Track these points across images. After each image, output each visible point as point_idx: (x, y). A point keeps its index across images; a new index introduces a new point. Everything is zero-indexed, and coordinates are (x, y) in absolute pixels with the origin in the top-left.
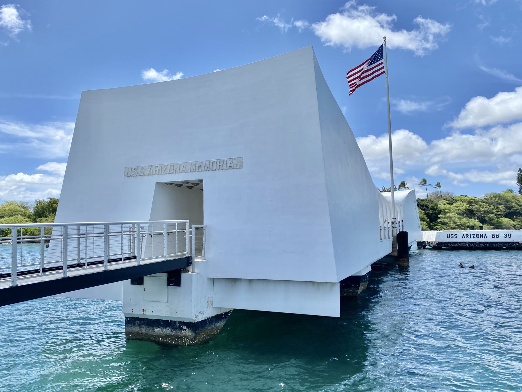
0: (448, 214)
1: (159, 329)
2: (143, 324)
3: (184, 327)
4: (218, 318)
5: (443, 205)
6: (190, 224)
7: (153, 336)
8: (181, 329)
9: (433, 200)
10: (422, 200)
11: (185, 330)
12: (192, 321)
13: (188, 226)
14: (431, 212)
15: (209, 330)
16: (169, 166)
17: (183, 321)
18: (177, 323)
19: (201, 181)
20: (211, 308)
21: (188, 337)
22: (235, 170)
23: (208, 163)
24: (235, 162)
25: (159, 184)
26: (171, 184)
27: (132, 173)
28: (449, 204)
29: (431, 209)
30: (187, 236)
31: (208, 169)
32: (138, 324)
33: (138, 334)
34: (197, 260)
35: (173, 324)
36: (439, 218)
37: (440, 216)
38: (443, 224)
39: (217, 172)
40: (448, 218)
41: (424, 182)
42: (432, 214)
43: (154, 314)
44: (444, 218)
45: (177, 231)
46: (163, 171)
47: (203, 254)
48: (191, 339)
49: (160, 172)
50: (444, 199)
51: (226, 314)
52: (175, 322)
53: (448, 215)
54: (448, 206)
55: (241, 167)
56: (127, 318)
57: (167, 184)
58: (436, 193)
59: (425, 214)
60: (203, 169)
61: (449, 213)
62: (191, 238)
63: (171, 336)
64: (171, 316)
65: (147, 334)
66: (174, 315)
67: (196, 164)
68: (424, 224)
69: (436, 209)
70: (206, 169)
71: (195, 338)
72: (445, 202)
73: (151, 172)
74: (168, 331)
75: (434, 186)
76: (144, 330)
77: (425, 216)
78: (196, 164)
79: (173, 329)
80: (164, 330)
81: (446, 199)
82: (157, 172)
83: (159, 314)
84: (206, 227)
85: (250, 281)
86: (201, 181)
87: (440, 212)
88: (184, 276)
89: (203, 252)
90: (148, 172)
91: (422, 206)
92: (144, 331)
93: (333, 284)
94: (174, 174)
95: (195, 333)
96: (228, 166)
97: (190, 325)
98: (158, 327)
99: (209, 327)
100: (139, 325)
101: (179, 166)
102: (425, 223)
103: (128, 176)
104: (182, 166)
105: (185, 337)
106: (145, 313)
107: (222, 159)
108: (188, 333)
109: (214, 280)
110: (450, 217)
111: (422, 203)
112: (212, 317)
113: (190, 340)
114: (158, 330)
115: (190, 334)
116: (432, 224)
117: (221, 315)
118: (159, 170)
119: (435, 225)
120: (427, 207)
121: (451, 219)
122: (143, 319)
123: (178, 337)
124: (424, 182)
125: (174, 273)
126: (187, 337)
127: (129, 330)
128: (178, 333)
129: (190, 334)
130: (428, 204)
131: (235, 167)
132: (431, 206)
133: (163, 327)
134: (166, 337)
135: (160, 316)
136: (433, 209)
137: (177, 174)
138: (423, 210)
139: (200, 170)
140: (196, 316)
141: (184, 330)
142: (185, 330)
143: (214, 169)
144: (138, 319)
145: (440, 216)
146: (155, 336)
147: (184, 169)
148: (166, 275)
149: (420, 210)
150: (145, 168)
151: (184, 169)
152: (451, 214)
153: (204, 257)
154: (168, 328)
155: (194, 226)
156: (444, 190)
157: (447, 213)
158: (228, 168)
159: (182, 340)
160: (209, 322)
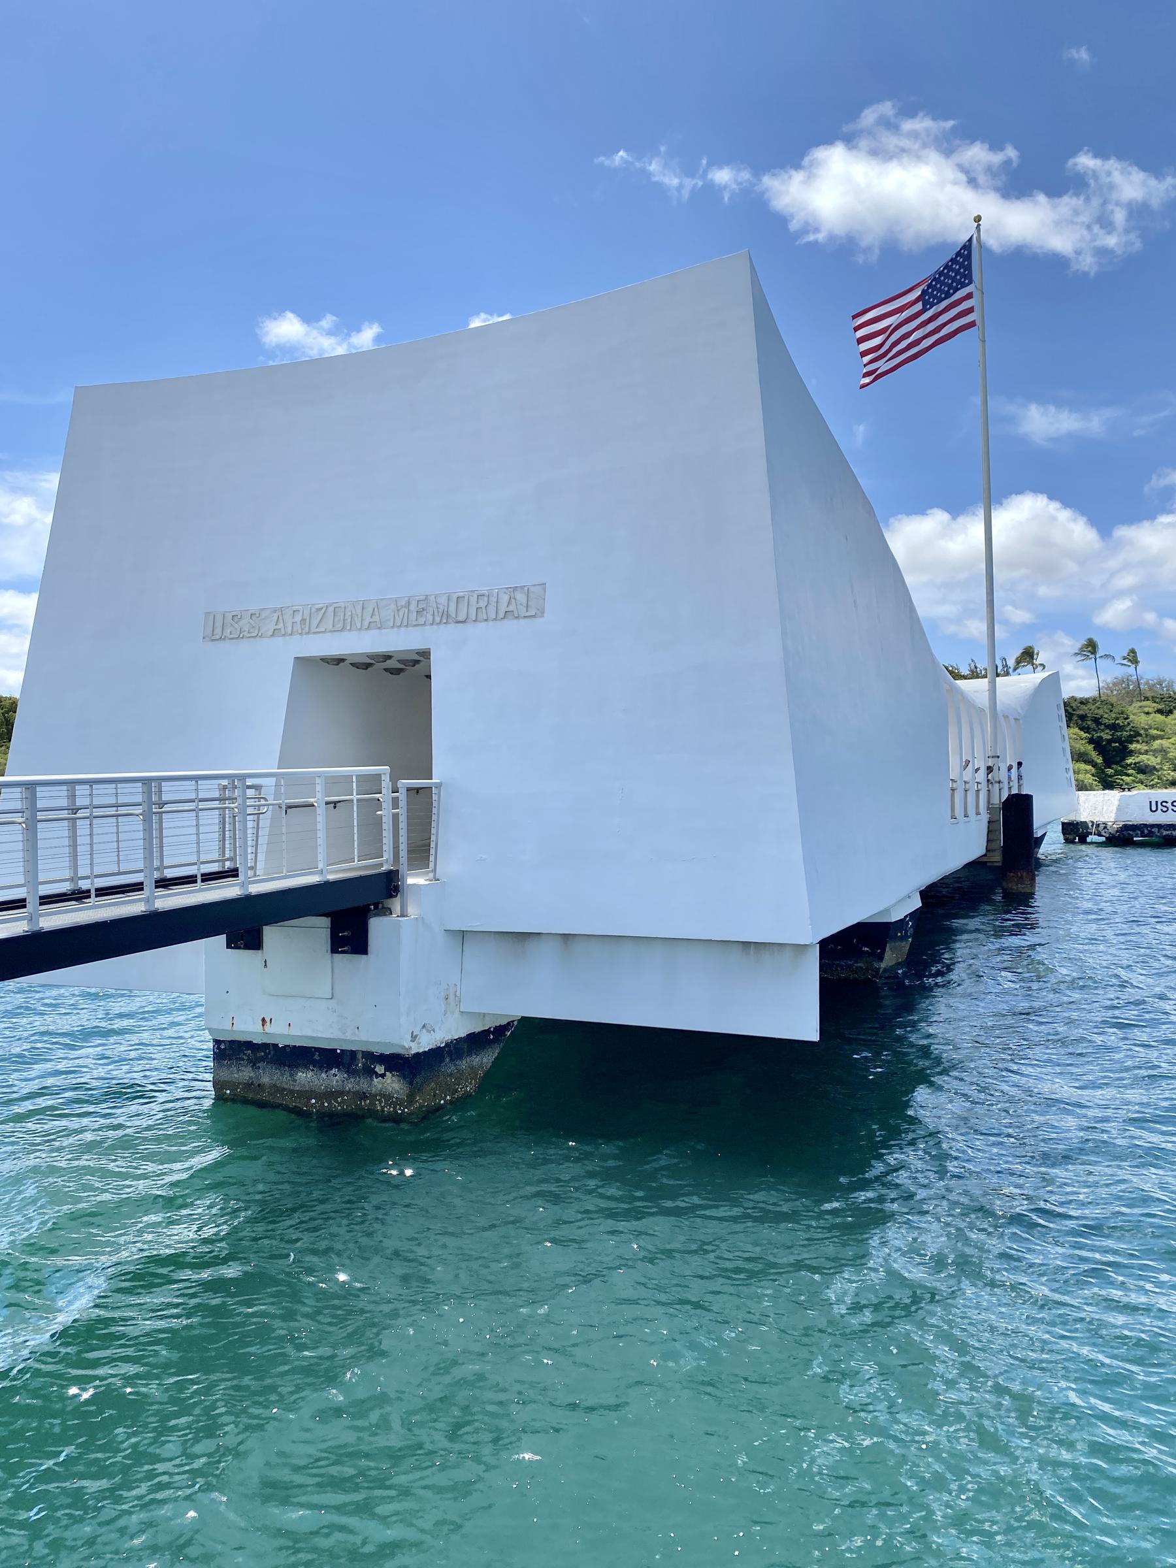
0: (1158, 742)
1: (310, 1074)
2: (262, 1059)
3: (380, 1069)
4: (475, 1042)
5: (1143, 718)
6: (394, 779)
7: (292, 1092)
8: (371, 1073)
9: (1113, 700)
10: (1084, 702)
11: (383, 1076)
12: (402, 1052)
13: (386, 784)
14: (1106, 735)
15: (451, 1075)
16: (331, 609)
17: (377, 1050)
18: (360, 1056)
19: (426, 654)
20: (457, 1014)
22: (522, 622)
23: (443, 600)
24: (521, 597)
26: (339, 661)
28: (1160, 711)
29: (1108, 727)
30: (386, 813)
31: (446, 618)
32: (250, 1061)
33: (249, 1085)
34: (414, 880)
35: (346, 1059)
36: (1131, 753)
37: (1133, 746)
38: (1143, 770)
39: (469, 628)
40: (1155, 752)
41: (1091, 647)
42: (1109, 742)
43: (295, 1031)
44: (1146, 752)
45: (355, 797)
46: (315, 623)
47: (432, 865)
48: (399, 1102)
49: (306, 628)
50: (1147, 699)
51: (500, 1030)
52: (353, 1054)
53: (1157, 744)
54: (1159, 717)
55: (541, 612)
56: (217, 1042)
57: (326, 660)
58: (1125, 681)
59: (1091, 741)
60: (430, 618)
61: (1162, 737)
62: (396, 817)
63: (341, 1093)
64: (341, 1036)
65: (275, 1085)
66: (349, 1036)
67: (409, 603)
68: (1086, 772)
69: (1122, 728)
70: (438, 619)
71: (411, 1098)
72: (1151, 706)
73: (281, 626)
74: (334, 1079)
75: (1118, 660)
76: (268, 1076)
77: (1091, 747)
79: (348, 1072)
80: (323, 1075)
81: (1154, 700)
82: (298, 627)
83: (308, 1032)
84: (438, 786)
85: (567, 938)
86: (426, 654)
87: (1135, 736)
88: (377, 926)
89: (432, 858)
90: (272, 627)
91: (1083, 717)
92: (265, 1080)
93: (800, 948)
94: (345, 634)
95: (411, 1083)
96: (503, 608)
97: (396, 1062)
98: (306, 1067)
99: (449, 1067)
100: (253, 1063)
102: (1089, 767)
103: (212, 637)
105: (380, 1095)
106: (268, 1028)
107: (484, 590)
108: (391, 1083)
109: (462, 936)
110: (1163, 751)
111: (1083, 710)
112: (459, 1040)
113: (395, 1104)
114: (305, 1077)
115: (396, 1086)
116: (1110, 771)
117: (487, 1032)
118: (303, 620)
119: (1117, 773)
120: (1097, 721)
121: (1165, 758)
122: (265, 1046)
123: (363, 1096)
124: (1091, 647)
125: (349, 915)
126: (387, 1097)
127: (225, 1075)
128: (362, 1084)
130: (1100, 712)
131: (523, 612)
132: (1109, 718)
133: (321, 1068)
134: (331, 1095)
136: (1114, 727)
138: (1086, 729)
139: (422, 620)
140: (414, 1038)
141: (378, 1075)
142: (383, 1076)
143: (460, 618)
144: (249, 1045)
145: (1133, 746)
147: (376, 618)
148: (325, 922)
149: (1076, 730)
151: (376, 618)
152: (1165, 743)
153: (434, 871)
155: (404, 783)
156: (1148, 671)
157: (1155, 738)
158: (501, 615)
160: (450, 1053)
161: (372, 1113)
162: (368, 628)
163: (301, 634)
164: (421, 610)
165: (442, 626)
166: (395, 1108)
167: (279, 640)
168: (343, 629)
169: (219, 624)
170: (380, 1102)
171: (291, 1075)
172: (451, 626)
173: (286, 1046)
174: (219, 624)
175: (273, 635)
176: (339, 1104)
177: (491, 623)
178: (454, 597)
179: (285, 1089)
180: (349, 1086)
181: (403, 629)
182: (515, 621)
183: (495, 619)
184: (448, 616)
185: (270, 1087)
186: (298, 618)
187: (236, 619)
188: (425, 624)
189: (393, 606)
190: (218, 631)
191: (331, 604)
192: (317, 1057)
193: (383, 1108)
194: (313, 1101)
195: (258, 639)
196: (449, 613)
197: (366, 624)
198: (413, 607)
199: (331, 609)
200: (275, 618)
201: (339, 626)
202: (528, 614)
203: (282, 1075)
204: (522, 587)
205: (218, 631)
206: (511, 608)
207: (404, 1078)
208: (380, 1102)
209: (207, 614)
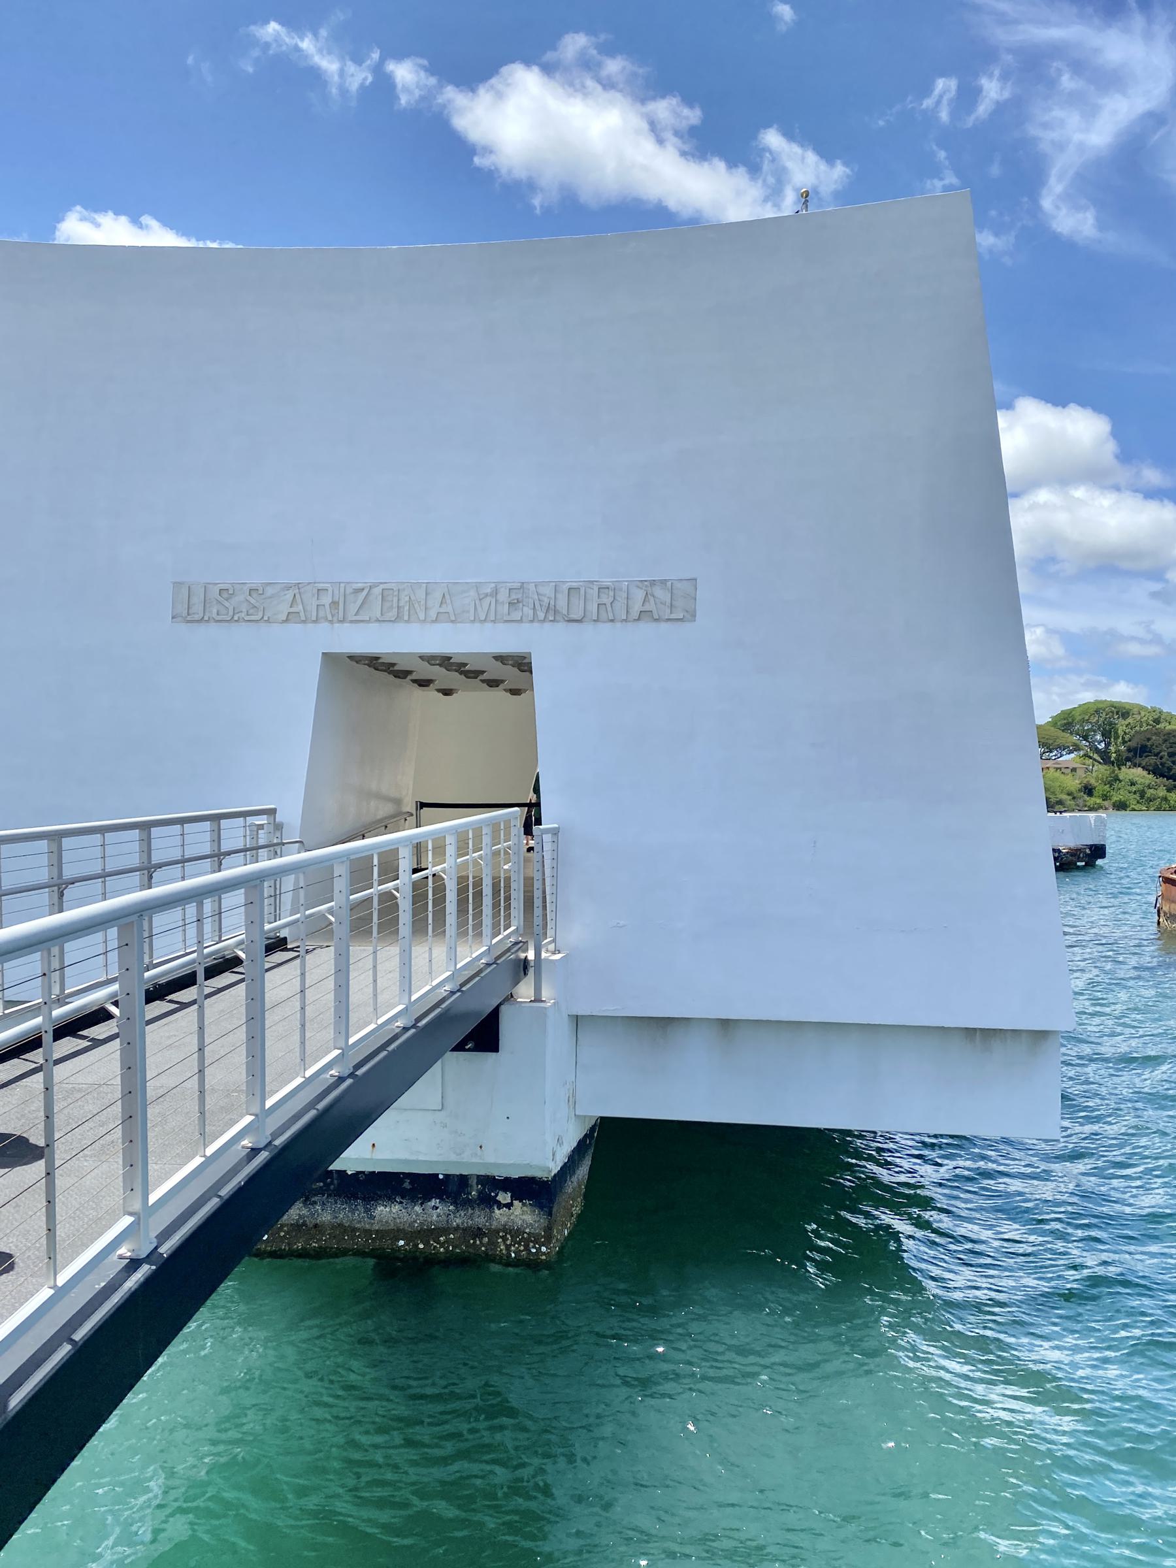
1: (396, 1208)
2: (320, 1192)
3: (504, 1197)
7: (368, 1232)
8: (488, 1202)
11: (509, 1206)
16: (377, 591)
17: (500, 1173)
21: (519, 1232)
22: (664, 626)
23: (548, 591)
25: (330, 659)
27: (207, 606)
31: (552, 613)
35: (452, 1188)
39: (588, 629)
46: (353, 608)
49: (337, 613)
51: (592, 1129)
52: (463, 1180)
55: (691, 616)
57: (355, 658)
60: (528, 611)
63: (445, 1231)
65: (340, 1225)
66: (467, 1157)
67: (495, 592)
70: (541, 615)
71: (548, 1229)
74: (435, 1212)
78: (495, 592)
79: (455, 1203)
80: (418, 1209)
90: (284, 609)
92: (326, 1217)
96: (637, 608)
97: (528, 1189)
98: (391, 1199)
101: (421, 594)
104: (438, 595)
105: (505, 1230)
107: (607, 581)
108: (522, 1215)
109: (577, 1020)
114: (388, 1213)
115: (529, 1218)
118: (334, 604)
123: (478, 1232)
126: (515, 1233)
128: (479, 1218)
129: (529, 1218)
135: (406, 1162)
137: (415, 627)
139: (516, 615)
141: (500, 1206)
142: (509, 1206)
146: (377, 1231)
150: (270, 591)
154: (433, 1202)
158: (635, 615)
159: (493, 1244)
161: (490, 1258)
162: (436, 621)
163: (331, 622)
164: (516, 601)
165: (547, 625)
166: (527, 1248)
167: (295, 628)
168: (398, 618)
169: (197, 600)
170: (504, 1239)
171: (367, 1211)
172: (561, 626)
173: (358, 1173)
174: (197, 600)
175: (287, 621)
176: (442, 1245)
177: (619, 625)
178: (565, 587)
179: (354, 1230)
180: (457, 1221)
181: (489, 625)
182: (654, 625)
183: (625, 620)
184: (556, 612)
185: (333, 1227)
186: (326, 600)
187: (225, 595)
188: (521, 621)
189: (473, 593)
190: (198, 608)
191: (376, 585)
192: (407, 1185)
193: (508, 1248)
194: (402, 1243)
195: (262, 624)
196: (560, 608)
197: (433, 614)
198: (503, 596)
199: (377, 591)
200: (289, 596)
201: (392, 614)
202: (673, 616)
203: (353, 1211)
204: (664, 582)
205: (198, 608)
206: (647, 608)
207: (541, 1207)
208: (504, 1239)
209: (177, 585)
